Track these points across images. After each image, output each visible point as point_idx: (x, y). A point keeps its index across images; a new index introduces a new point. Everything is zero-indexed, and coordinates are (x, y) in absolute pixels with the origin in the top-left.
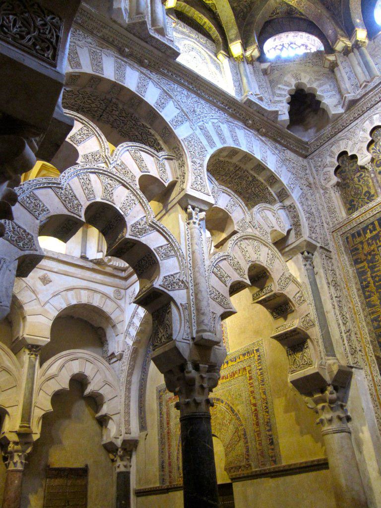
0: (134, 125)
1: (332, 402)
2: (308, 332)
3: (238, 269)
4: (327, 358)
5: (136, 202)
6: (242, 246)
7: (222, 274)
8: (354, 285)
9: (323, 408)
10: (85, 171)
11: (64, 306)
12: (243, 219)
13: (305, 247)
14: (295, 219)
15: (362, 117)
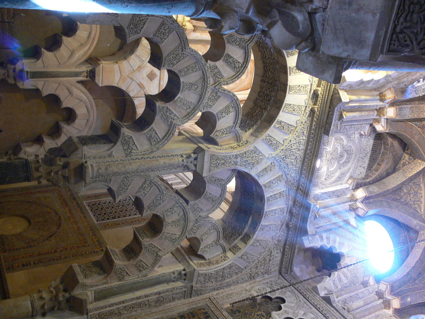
0: (262, 108)
1: (56, 296)
2: (112, 274)
3: (155, 204)
4: (93, 292)
5: (188, 110)
6: (176, 208)
7: (145, 189)
8: (161, 316)
9: (52, 292)
10: (202, 67)
11: (132, 94)
12: (202, 210)
13: (189, 270)
14: (215, 262)
15: (317, 312)
